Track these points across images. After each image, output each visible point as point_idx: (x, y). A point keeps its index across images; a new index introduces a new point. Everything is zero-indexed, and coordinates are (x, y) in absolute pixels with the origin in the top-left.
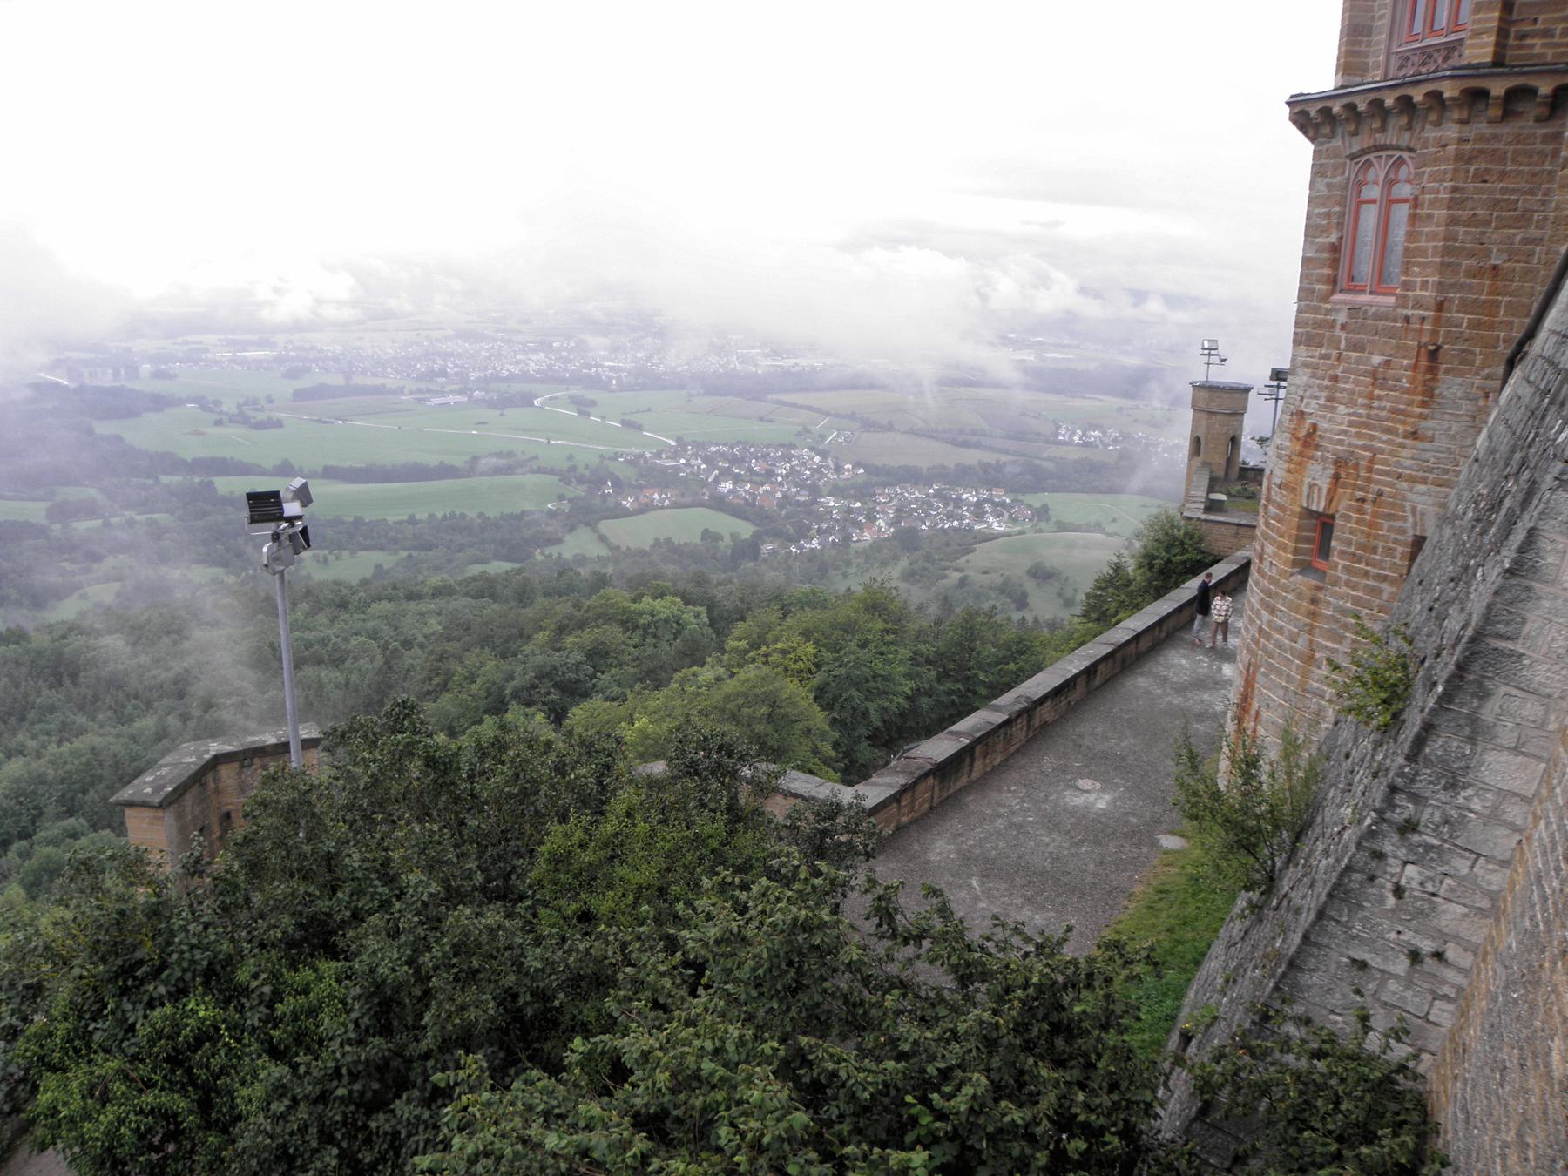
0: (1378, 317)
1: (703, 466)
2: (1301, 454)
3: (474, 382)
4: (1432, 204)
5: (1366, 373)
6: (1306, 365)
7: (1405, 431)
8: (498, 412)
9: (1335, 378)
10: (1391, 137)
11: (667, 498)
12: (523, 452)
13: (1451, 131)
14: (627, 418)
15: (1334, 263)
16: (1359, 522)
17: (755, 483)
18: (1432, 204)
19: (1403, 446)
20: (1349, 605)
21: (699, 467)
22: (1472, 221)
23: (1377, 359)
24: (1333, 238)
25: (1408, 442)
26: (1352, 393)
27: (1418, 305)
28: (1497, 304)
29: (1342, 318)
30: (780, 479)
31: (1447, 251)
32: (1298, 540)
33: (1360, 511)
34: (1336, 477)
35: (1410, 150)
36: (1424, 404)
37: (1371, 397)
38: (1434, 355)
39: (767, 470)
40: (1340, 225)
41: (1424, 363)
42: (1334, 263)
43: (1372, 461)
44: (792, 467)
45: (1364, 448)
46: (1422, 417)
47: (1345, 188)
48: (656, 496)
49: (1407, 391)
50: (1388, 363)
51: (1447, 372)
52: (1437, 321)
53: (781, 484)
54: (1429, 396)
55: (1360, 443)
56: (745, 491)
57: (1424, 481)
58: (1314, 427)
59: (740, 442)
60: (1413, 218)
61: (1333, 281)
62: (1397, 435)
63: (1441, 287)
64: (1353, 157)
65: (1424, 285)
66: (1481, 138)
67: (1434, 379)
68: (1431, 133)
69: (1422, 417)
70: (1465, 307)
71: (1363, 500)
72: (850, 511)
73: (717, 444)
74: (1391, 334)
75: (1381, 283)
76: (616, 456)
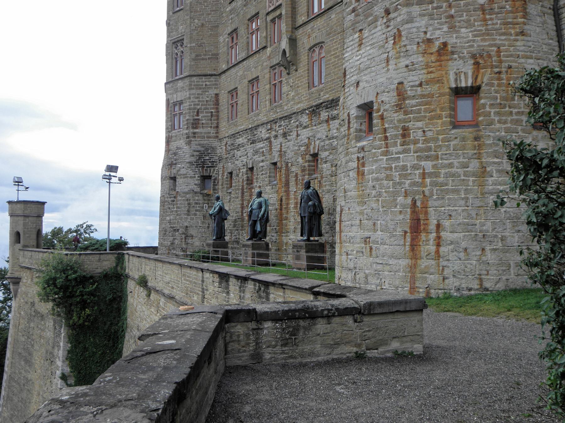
2: (438, 61)
7: (515, 32)
16: (499, 85)
19: (517, 40)
20: (503, 133)
25: (519, 37)
33: (499, 79)
45: (491, 46)
46: (524, 24)
55: (487, 43)
57: (531, 58)
62: (511, 35)
71: (500, 73)
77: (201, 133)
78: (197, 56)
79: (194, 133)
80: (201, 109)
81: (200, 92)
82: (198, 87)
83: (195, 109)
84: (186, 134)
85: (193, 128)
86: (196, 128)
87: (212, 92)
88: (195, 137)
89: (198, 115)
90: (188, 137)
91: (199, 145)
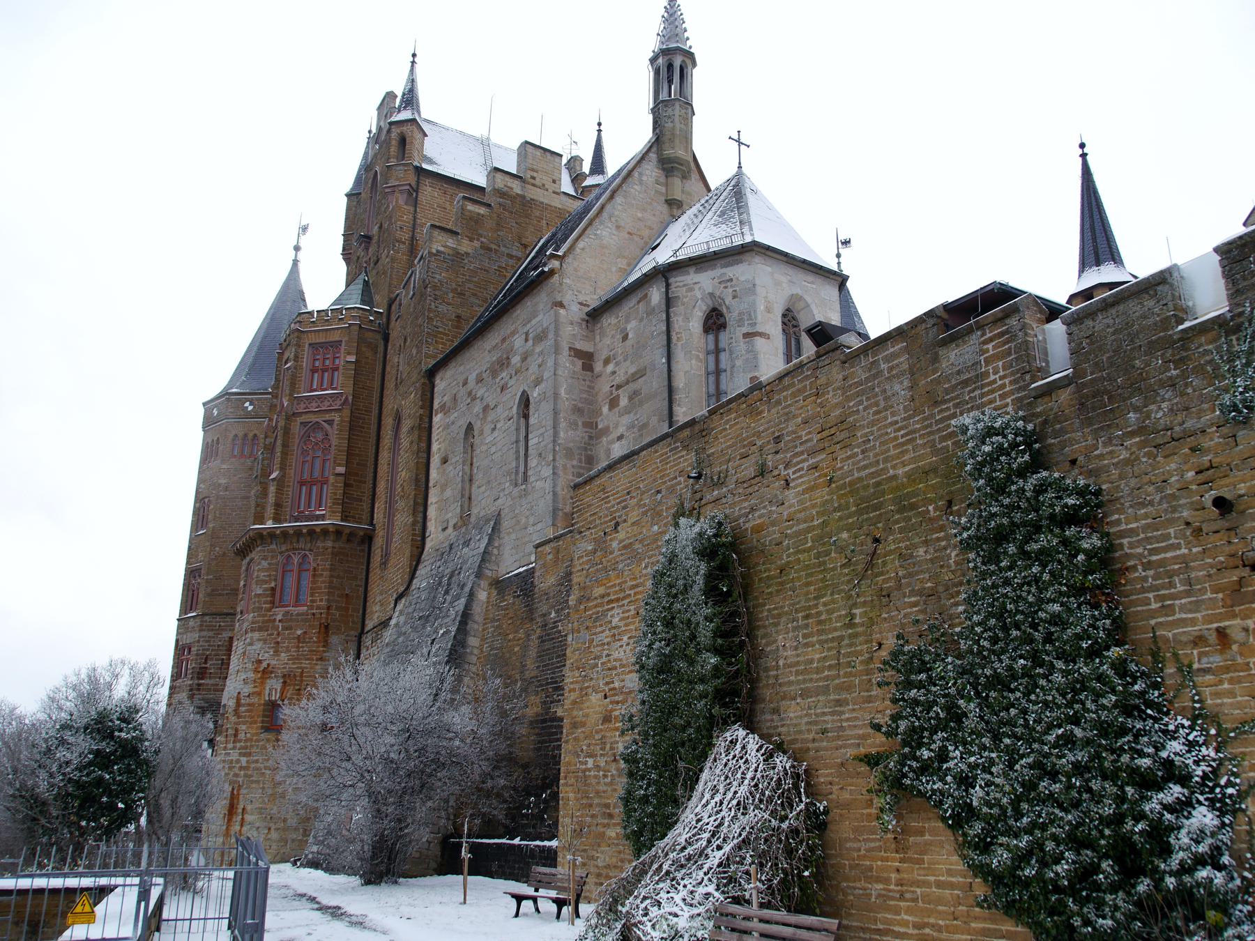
0: (298, 615)
4: (322, 570)
5: (294, 638)
6: (259, 640)
9: (278, 643)
10: (301, 545)
13: (329, 544)
15: (273, 595)
18: (322, 570)
22: (338, 577)
23: (299, 632)
24: (273, 585)
26: (288, 647)
27: (318, 608)
28: (348, 609)
29: (279, 617)
31: (330, 587)
32: (264, 716)
34: (284, 683)
35: (310, 550)
36: (324, 646)
37: (298, 647)
38: (327, 627)
40: (275, 580)
41: (323, 630)
42: (273, 595)
43: (302, 672)
45: (298, 668)
46: (324, 651)
47: (277, 564)
49: (314, 642)
50: (305, 633)
51: (333, 633)
52: (328, 614)
54: (326, 644)
58: (268, 665)
60: (314, 576)
61: (273, 602)
63: (328, 600)
64: (281, 553)
65: (321, 600)
66: (340, 548)
67: (327, 636)
68: (320, 544)
69: (324, 651)
70: (337, 609)
74: (306, 620)
75: (297, 603)
77: (207, 684)
78: (213, 590)
79: (199, 685)
80: (210, 655)
81: (211, 634)
82: (210, 628)
83: (203, 654)
84: (190, 685)
85: (199, 678)
86: (202, 679)
87: (226, 635)
88: (199, 690)
89: (206, 662)
90: (191, 690)
91: (203, 699)
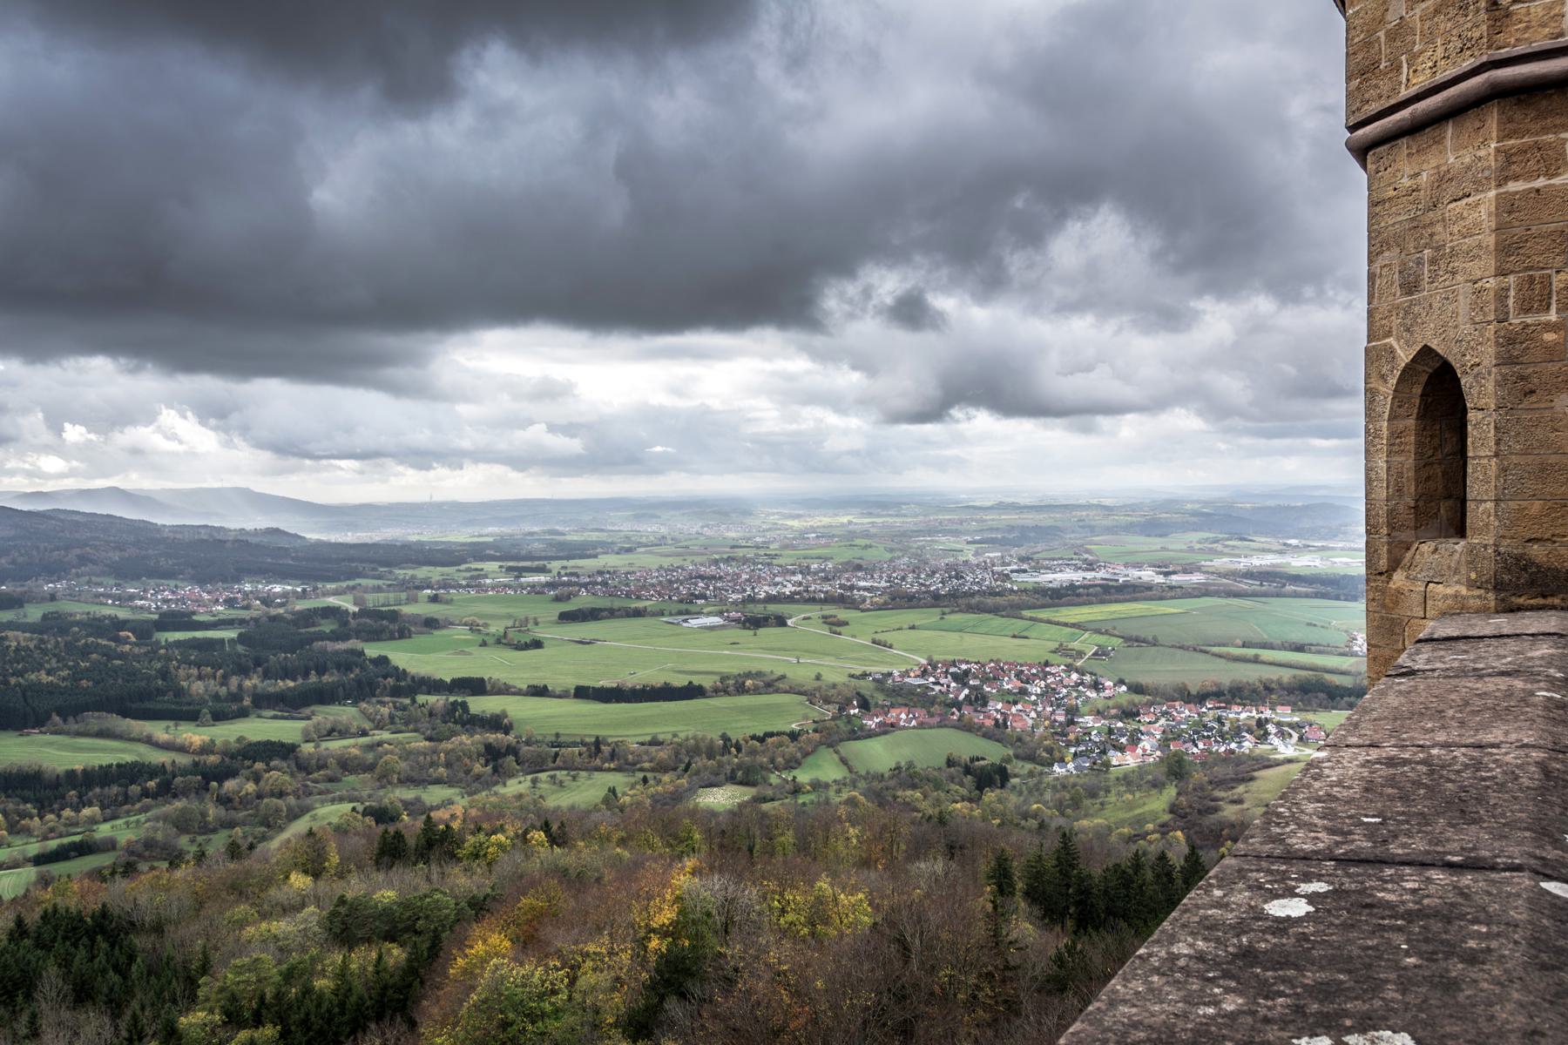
1: (953, 685)
3: (733, 603)
8: (752, 632)
11: (914, 717)
12: (772, 672)
14: (878, 637)
17: (1008, 702)
21: (948, 686)
30: (1033, 698)
39: (1020, 688)
44: (1047, 686)
48: (903, 716)
53: (1035, 703)
56: (997, 711)
59: (992, 661)
72: (1110, 731)
73: (967, 663)
76: (865, 675)
